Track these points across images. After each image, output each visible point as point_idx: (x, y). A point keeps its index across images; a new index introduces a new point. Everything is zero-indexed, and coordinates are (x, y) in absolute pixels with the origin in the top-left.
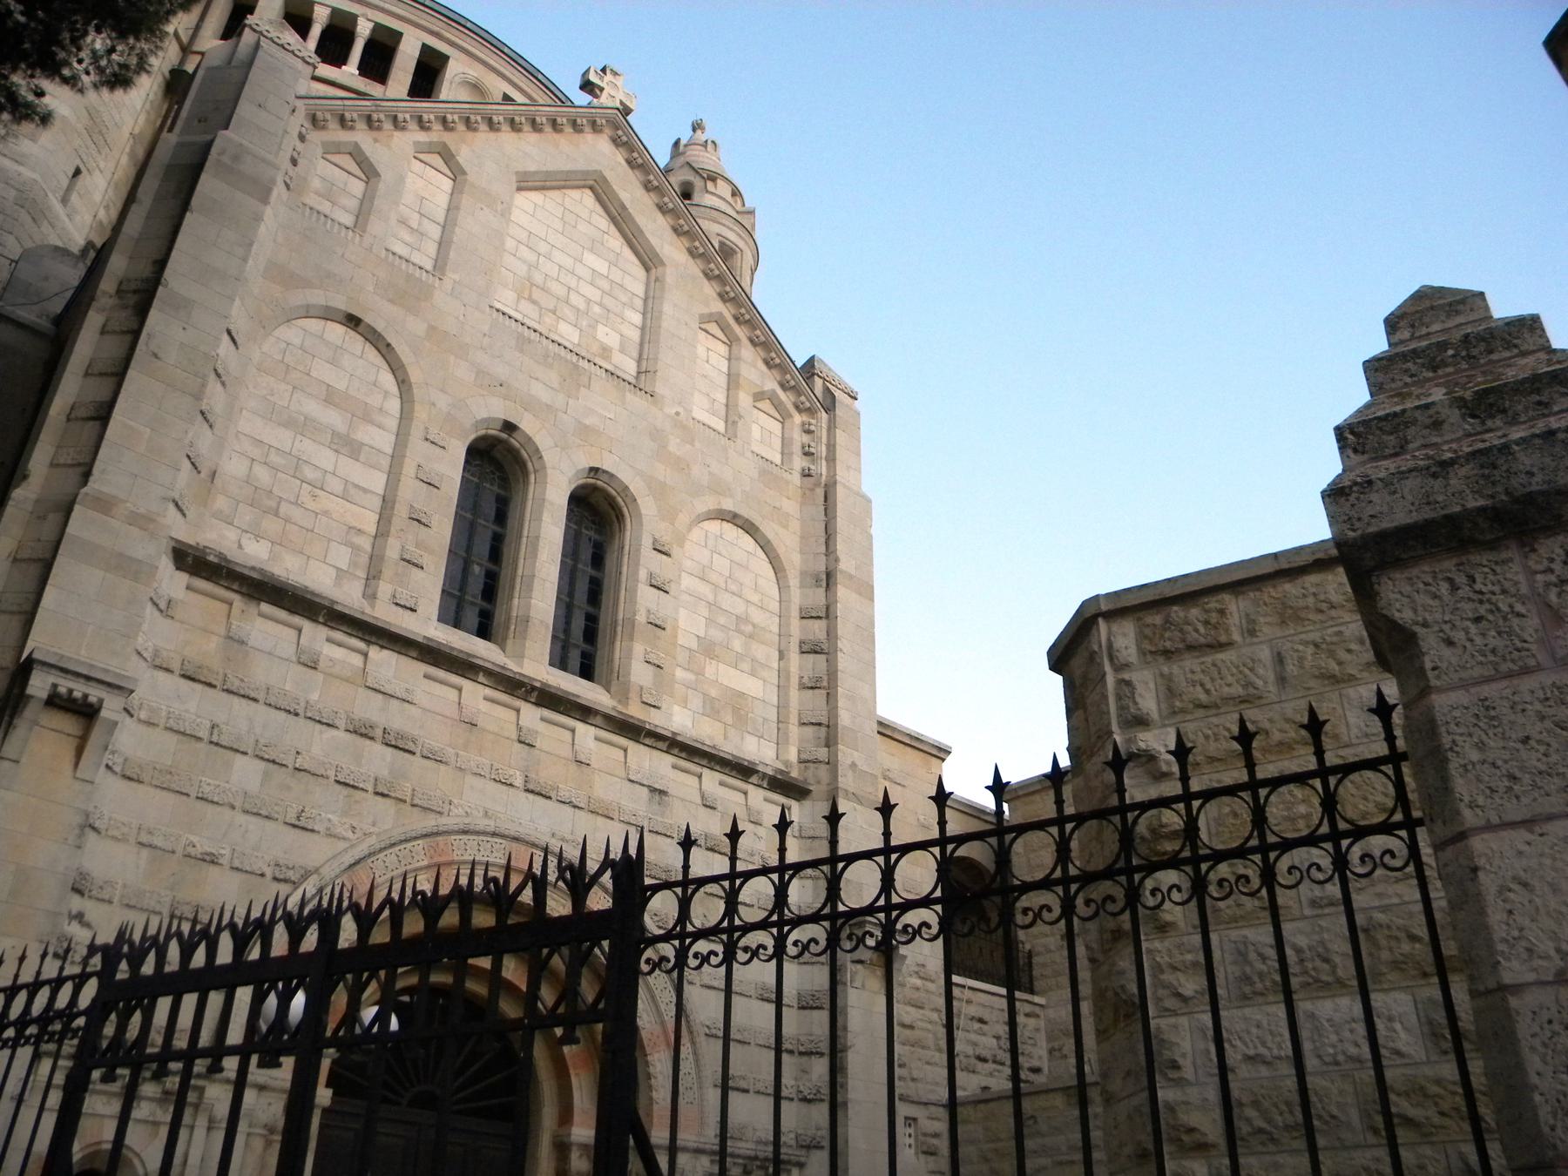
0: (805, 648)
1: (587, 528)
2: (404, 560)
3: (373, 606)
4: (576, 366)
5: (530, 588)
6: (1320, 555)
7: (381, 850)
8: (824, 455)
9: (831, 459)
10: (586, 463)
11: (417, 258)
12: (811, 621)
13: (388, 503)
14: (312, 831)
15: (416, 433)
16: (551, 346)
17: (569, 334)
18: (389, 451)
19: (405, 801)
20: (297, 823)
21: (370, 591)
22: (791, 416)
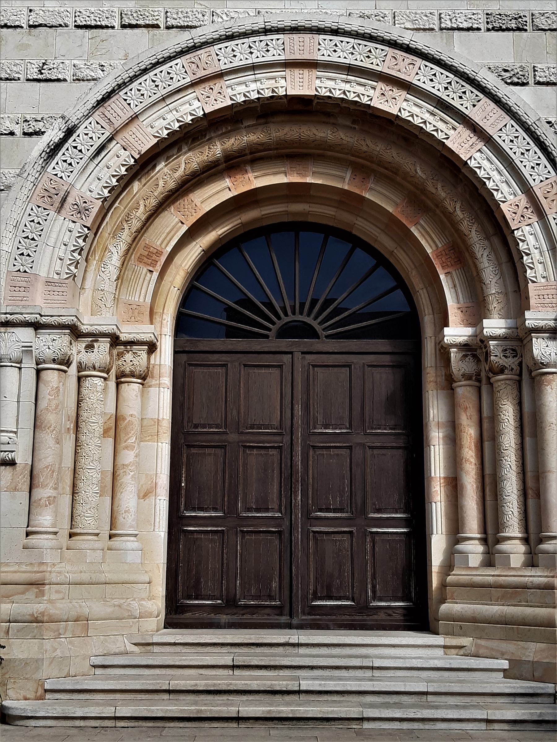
7: (133, 79)
14: (58, 80)
19: (157, 26)
20: (40, 76)
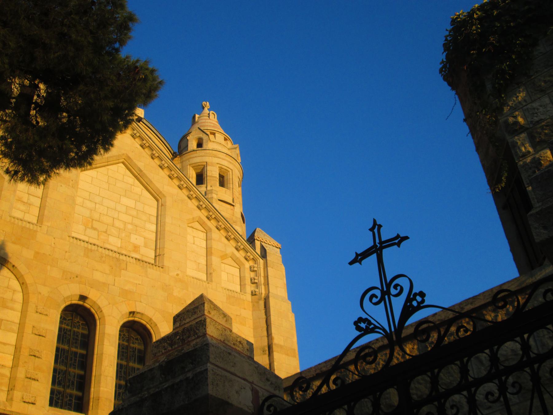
1: (133, 343)
2: (27, 378)
3: (11, 405)
4: (118, 260)
5: (99, 382)
6: (318, 371)
8: (263, 281)
9: (267, 284)
10: (125, 309)
11: (28, 218)
13: (18, 348)
15: (31, 308)
16: (104, 251)
17: (114, 242)
18: (18, 321)
21: (10, 397)
22: (243, 265)
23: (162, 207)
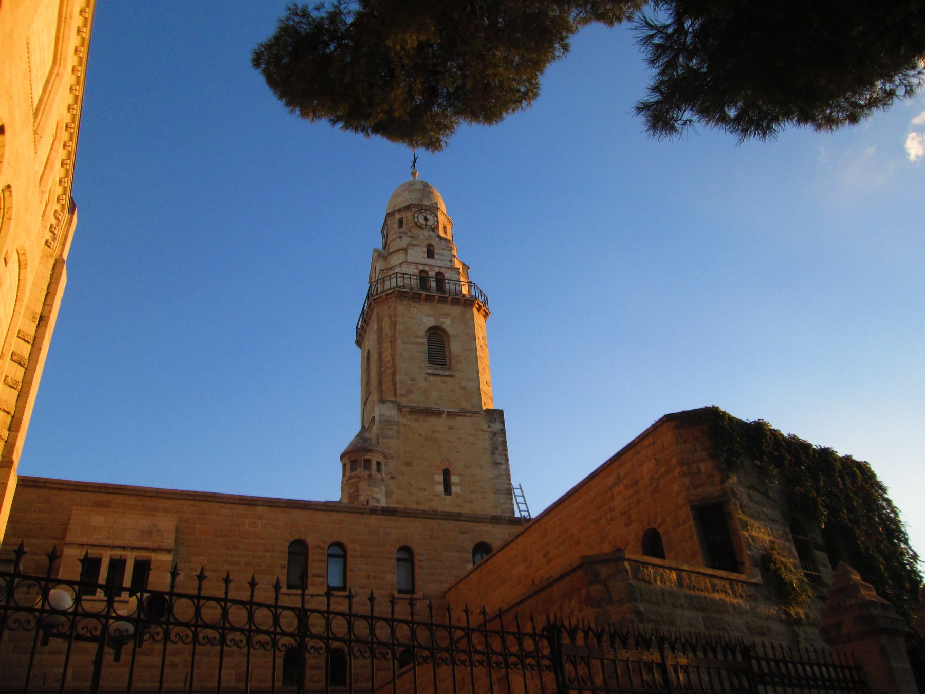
0: (15, 358)
12: (23, 342)
23: (57, 77)
